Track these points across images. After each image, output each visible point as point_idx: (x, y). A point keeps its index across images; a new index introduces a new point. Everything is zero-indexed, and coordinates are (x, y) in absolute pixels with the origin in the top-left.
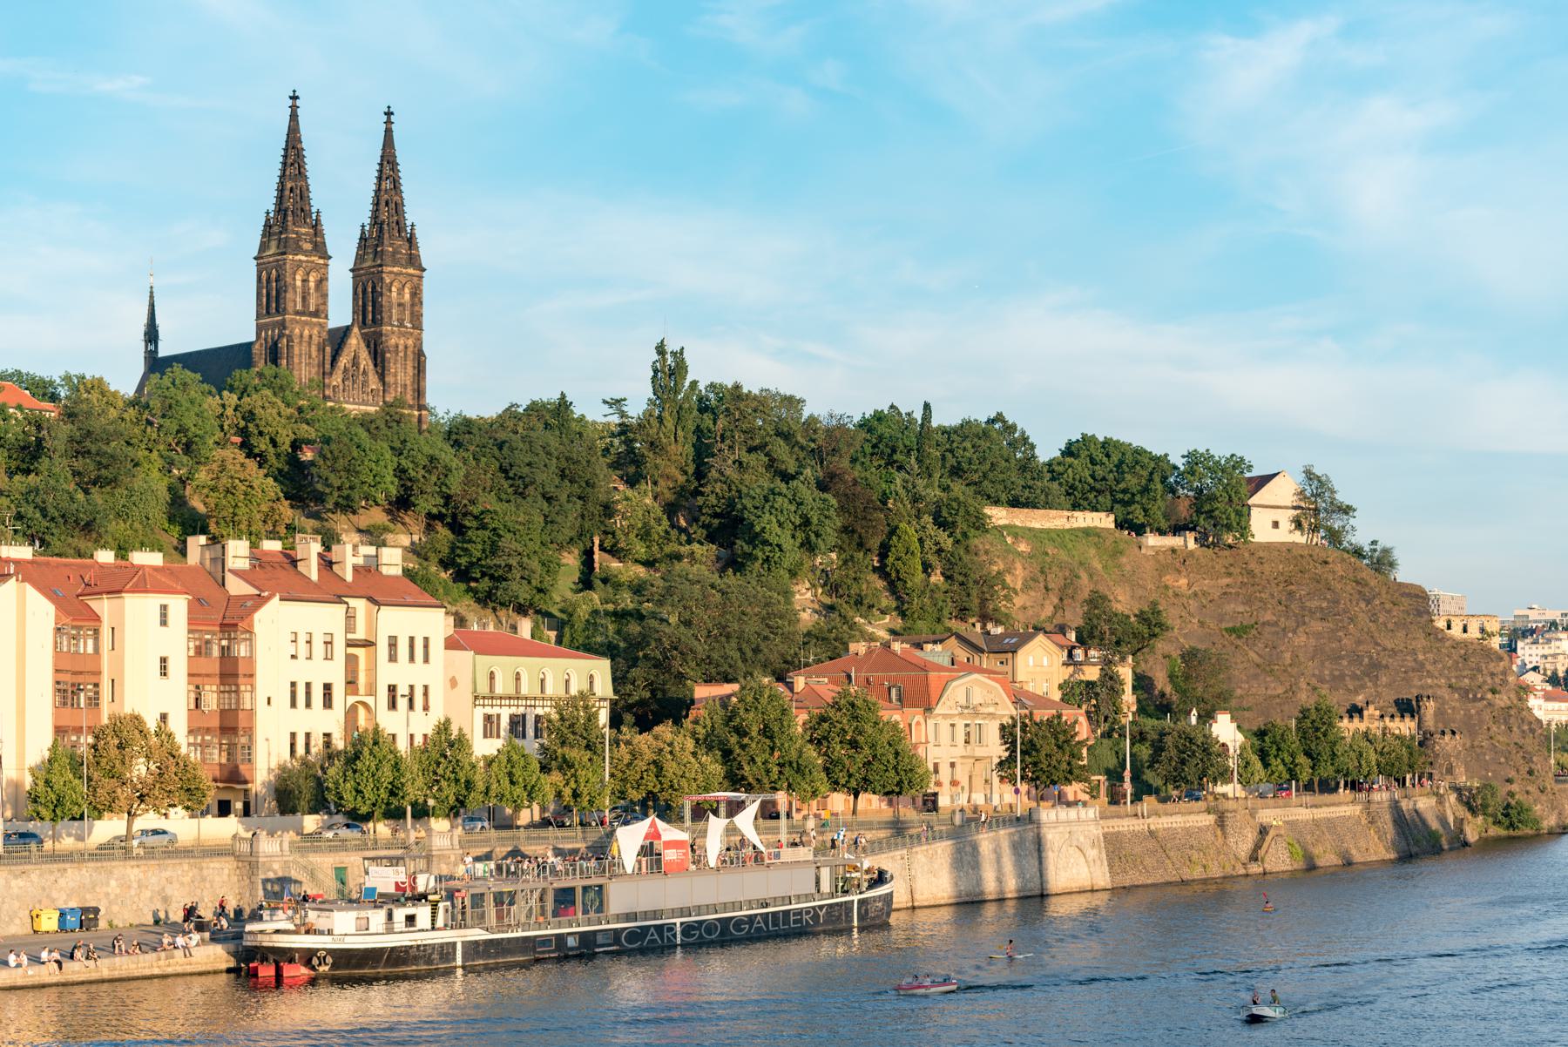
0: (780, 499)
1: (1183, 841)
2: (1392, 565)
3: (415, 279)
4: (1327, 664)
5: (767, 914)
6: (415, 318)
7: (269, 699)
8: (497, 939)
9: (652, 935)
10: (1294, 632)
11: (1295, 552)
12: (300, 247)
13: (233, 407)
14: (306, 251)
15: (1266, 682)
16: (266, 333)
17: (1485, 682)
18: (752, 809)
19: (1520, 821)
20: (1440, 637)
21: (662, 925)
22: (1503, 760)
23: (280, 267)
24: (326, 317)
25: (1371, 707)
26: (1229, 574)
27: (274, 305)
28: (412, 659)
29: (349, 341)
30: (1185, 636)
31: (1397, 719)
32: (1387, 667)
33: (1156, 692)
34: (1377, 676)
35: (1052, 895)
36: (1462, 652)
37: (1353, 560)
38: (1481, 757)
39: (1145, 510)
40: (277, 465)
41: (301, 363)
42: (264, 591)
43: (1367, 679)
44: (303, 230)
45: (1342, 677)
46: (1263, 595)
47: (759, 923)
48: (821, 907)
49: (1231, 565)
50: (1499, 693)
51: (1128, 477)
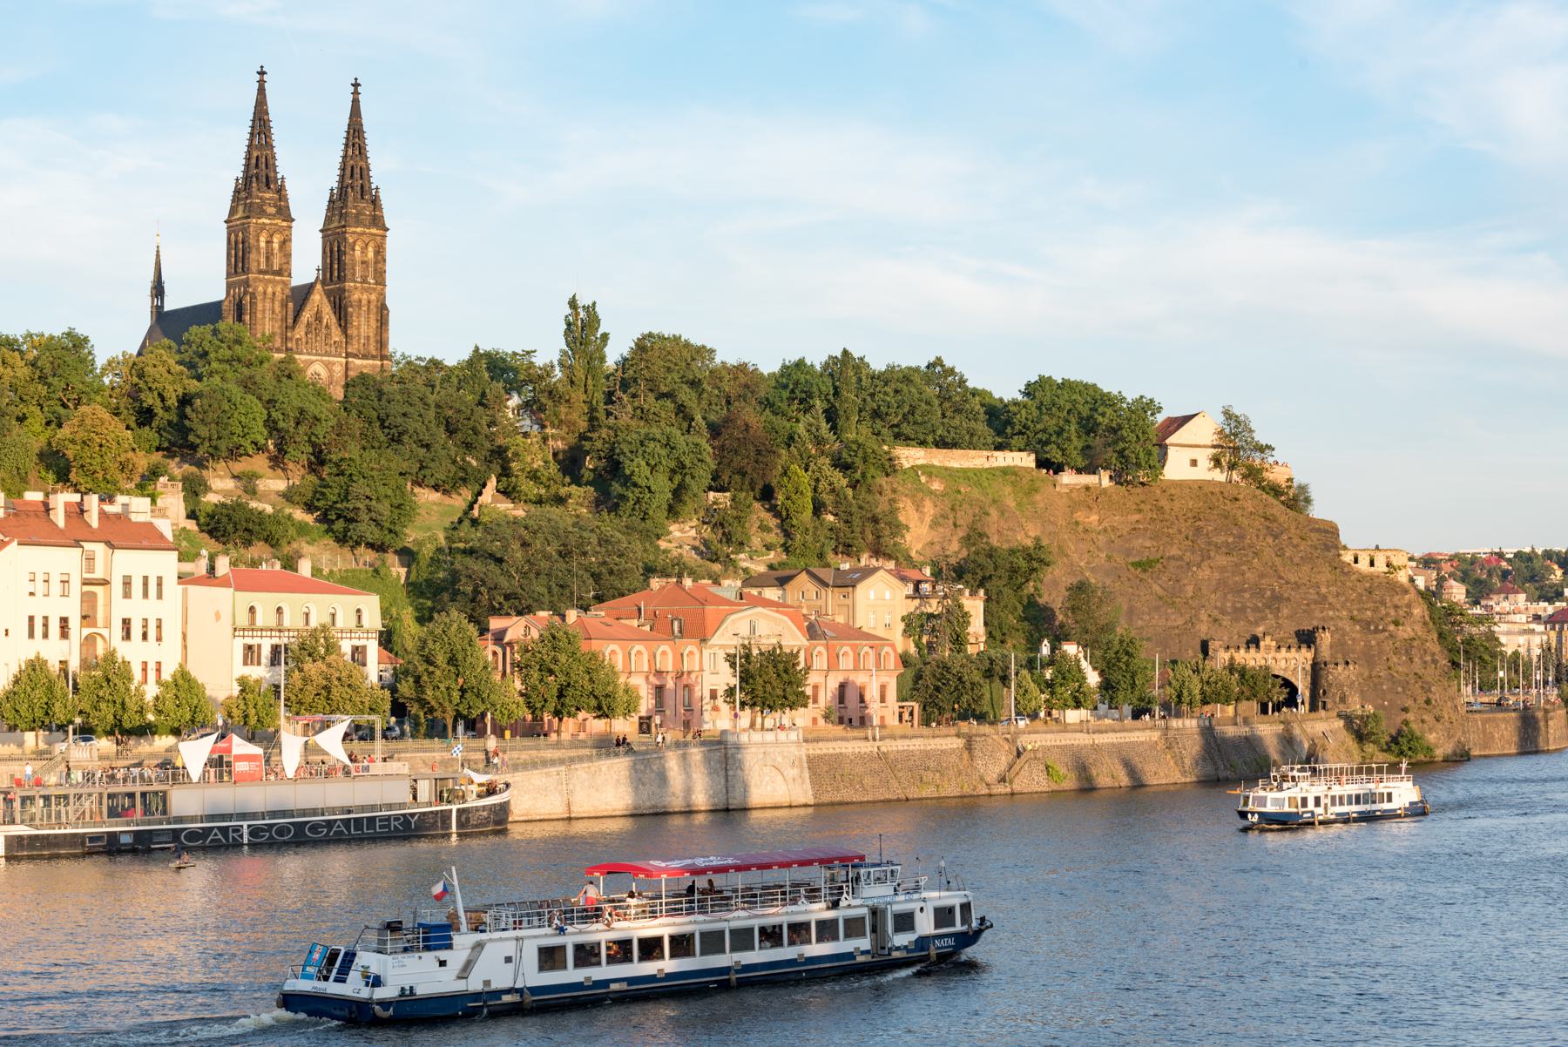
0: (652, 444)
1: (918, 763)
2: (1308, 501)
3: (378, 238)
4: (1229, 596)
5: (349, 819)
6: (378, 275)
7: (7, 631)
8: (43, 835)
9: (216, 835)
10: (1199, 566)
11: (1206, 490)
12: (264, 211)
13: (130, 365)
14: (270, 215)
15: (1166, 614)
16: (234, 291)
17: (1387, 614)
18: (340, 728)
19: (1410, 749)
20: (1346, 570)
21: (228, 827)
22: (1400, 689)
23: (245, 230)
24: (290, 275)
25: (1268, 638)
26: (1140, 511)
27: (240, 265)
28: (146, 595)
29: (312, 297)
30: (1093, 570)
31: (1293, 650)
32: (1288, 599)
33: (1057, 623)
34: (1278, 609)
35: (755, 809)
36: (1368, 585)
37: (1265, 496)
38: (1379, 687)
39: (1063, 450)
40: (167, 416)
41: (265, 318)
42: (6, 537)
43: (1267, 611)
44: (267, 195)
45: (1243, 609)
46: (1170, 531)
47: (339, 827)
48: (413, 815)
49: (1143, 502)
50: (1403, 625)
51: (1045, 418)
